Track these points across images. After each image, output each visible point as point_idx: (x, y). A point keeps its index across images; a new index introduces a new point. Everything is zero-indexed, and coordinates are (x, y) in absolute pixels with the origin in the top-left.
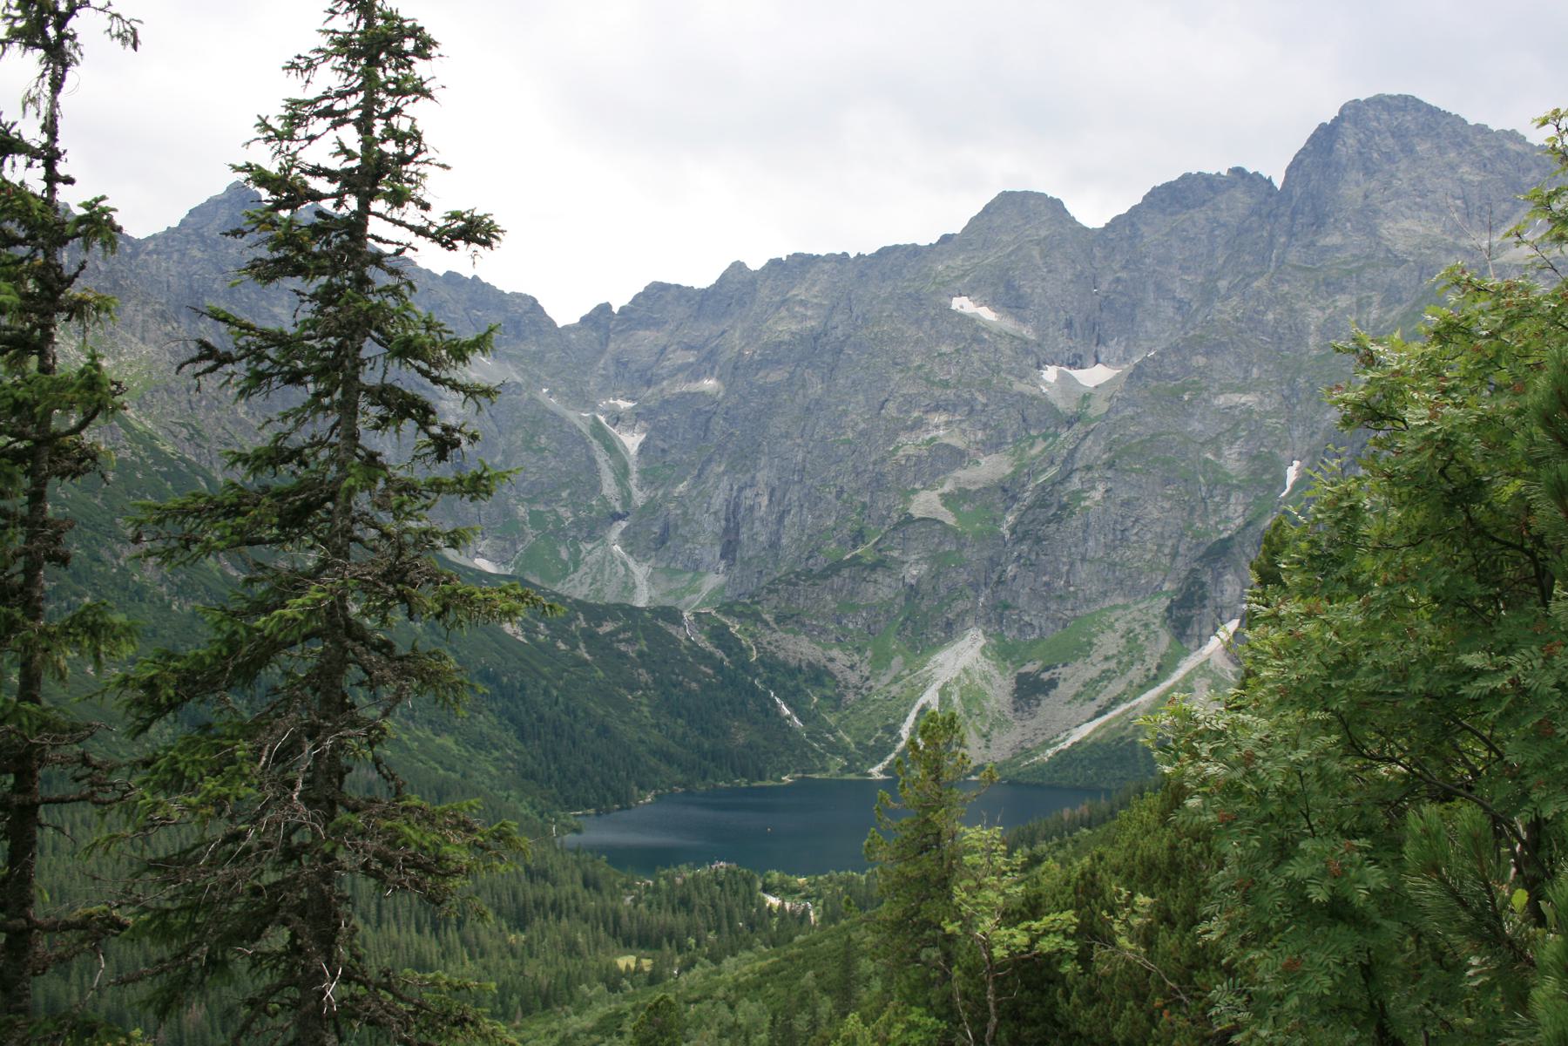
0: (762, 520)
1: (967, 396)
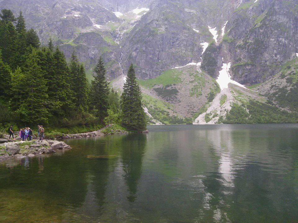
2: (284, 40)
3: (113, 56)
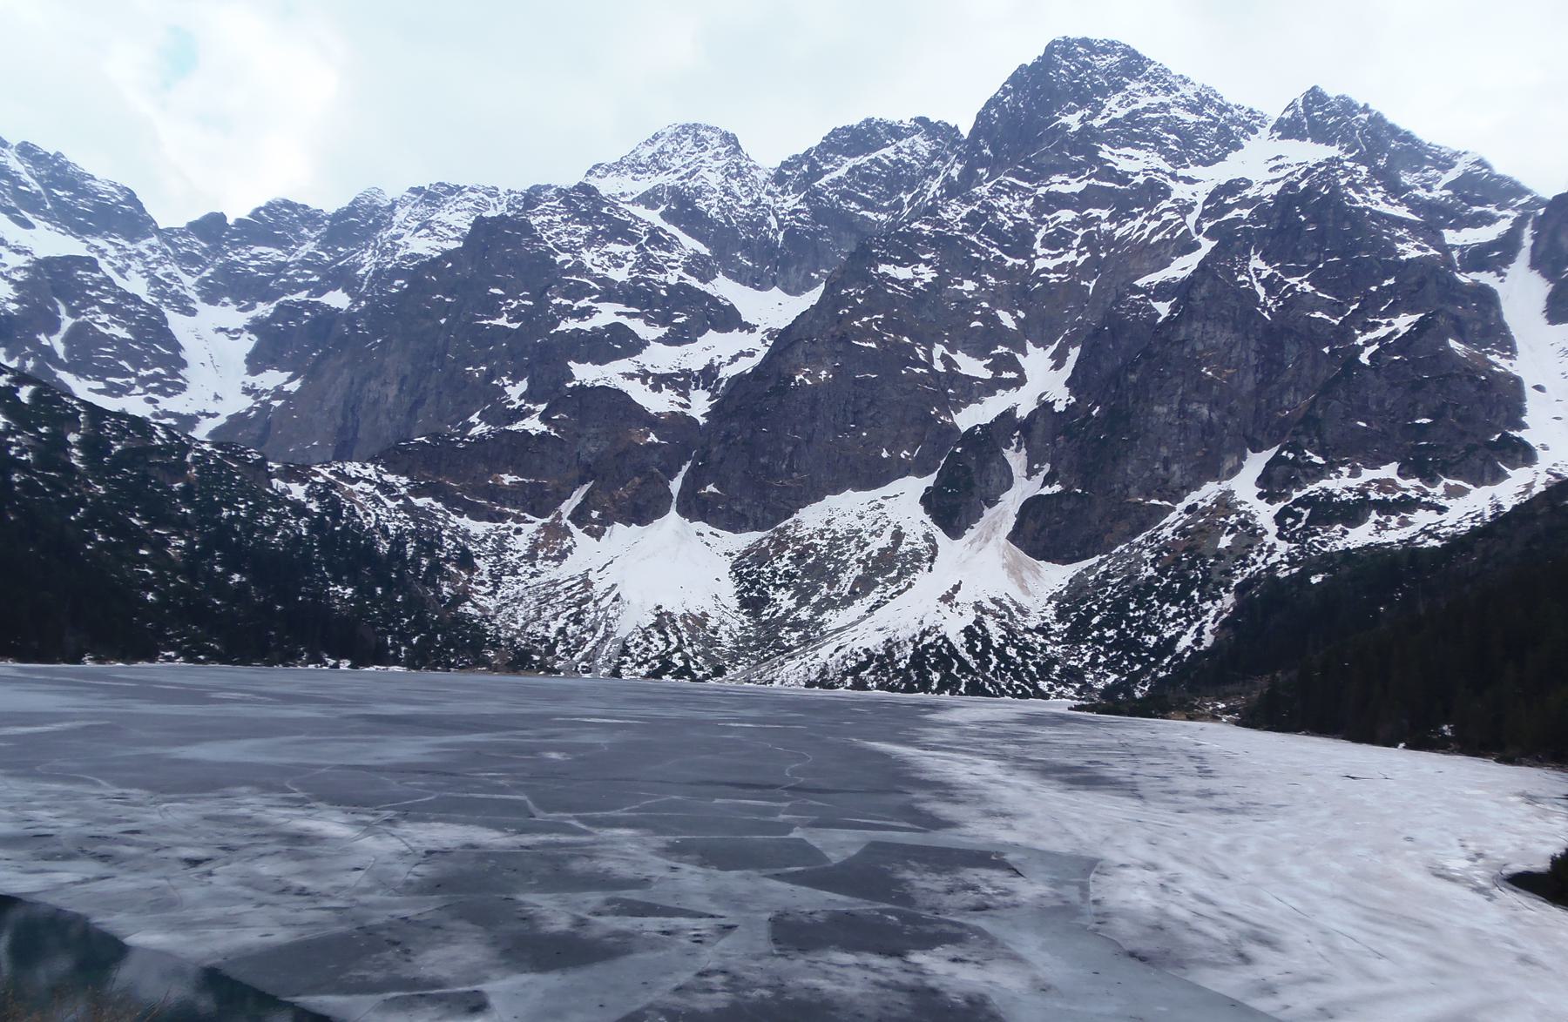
0: (388, 412)
2: (1205, 411)
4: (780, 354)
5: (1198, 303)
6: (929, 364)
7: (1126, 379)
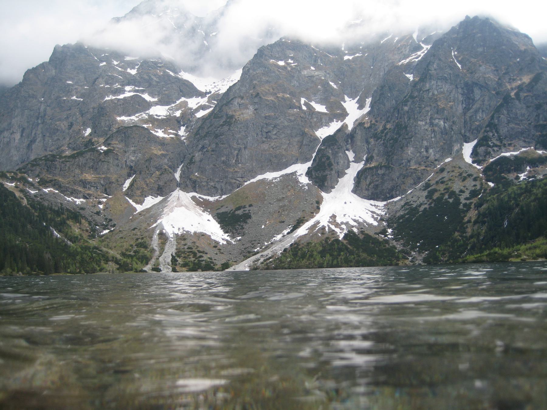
1: (146, 77)
2: (442, 123)
3: (166, 161)
4: (226, 105)
5: (433, 72)
6: (300, 108)
7: (402, 109)
